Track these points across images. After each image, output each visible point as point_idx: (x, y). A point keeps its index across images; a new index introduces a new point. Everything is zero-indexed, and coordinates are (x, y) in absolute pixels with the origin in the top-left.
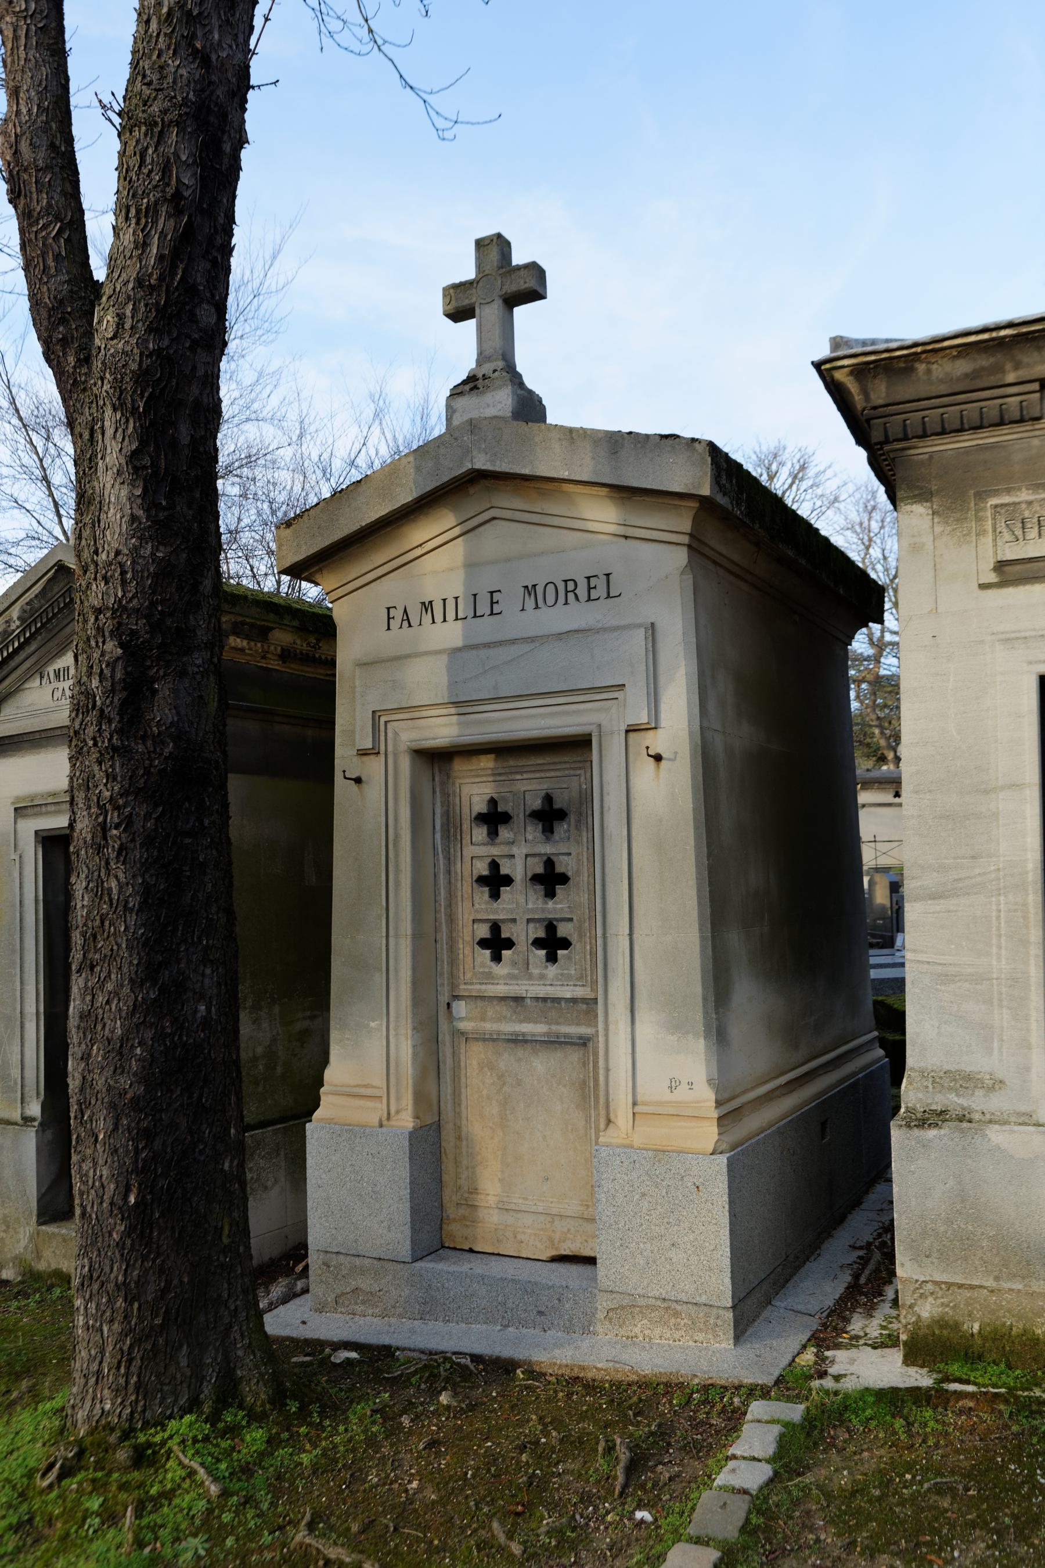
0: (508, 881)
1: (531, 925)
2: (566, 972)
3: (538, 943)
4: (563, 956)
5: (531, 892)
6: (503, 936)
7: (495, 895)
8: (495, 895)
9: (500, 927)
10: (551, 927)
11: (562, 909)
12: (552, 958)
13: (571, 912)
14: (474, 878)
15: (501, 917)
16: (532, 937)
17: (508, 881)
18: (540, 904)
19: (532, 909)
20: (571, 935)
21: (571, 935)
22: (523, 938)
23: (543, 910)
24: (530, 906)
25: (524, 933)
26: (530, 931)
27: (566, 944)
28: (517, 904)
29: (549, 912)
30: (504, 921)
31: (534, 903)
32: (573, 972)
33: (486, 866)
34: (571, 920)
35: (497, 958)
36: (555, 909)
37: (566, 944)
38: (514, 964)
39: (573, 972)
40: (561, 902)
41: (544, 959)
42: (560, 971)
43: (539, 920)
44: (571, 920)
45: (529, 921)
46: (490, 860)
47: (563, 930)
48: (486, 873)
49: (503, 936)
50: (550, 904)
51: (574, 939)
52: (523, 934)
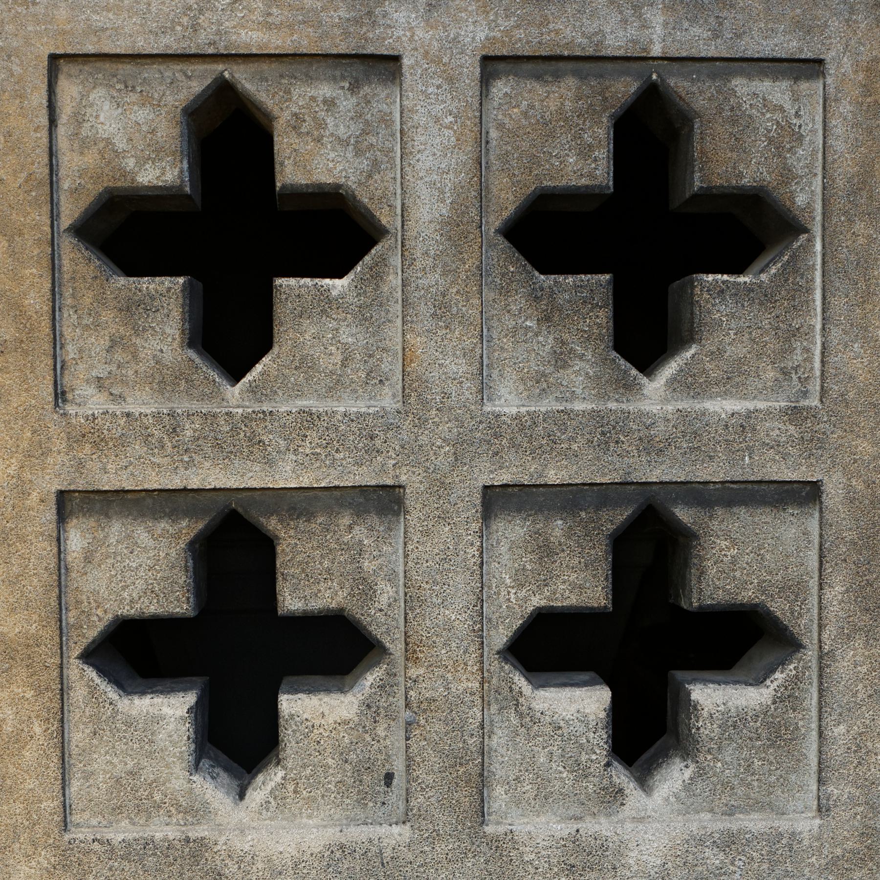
0: (336, 233)
1: (511, 530)
2: (755, 823)
3: (546, 646)
4: (734, 723)
5: (515, 313)
6: (291, 602)
7: (232, 336)
8: (232, 336)
9: (266, 546)
10: (648, 541)
11: (745, 424)
12: (644, 734)
13: (813, 445)
14: (70, 211)
15: (287, 476)
16: (514, 604)
17: (336, 233)
18: (583, 383)
19: (525, 425)
20: (794, 590)
21: (794, 590)
22: (456, 614)
23: (607, 432)
24: (508, 402)
25: (461, 584)
26: (502, 572)
27: (744, 638)
28: (411, 387)
29: (651, 447)
30: (301, 503)
31: (539, 383)
32: (807, 824)
33: (168, 131)
34: (808, 494)
35: (238, 741)
36: (692, 428)
37: (744, 638)
38: (374, 782)
39: (807, 824)
40: (731, 381)
41: (599, 741)
42: (718, 825)
43: (569, 499)
44: (808, 494)
45: (496, 501)
46: (194, 83)
47: (731, 563)
48: (162, 170)
49: (291, 602)
50: (655, 394)
51: (820, 610)
52: (446, 585)
